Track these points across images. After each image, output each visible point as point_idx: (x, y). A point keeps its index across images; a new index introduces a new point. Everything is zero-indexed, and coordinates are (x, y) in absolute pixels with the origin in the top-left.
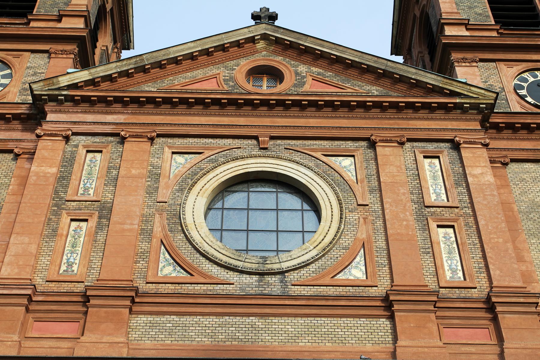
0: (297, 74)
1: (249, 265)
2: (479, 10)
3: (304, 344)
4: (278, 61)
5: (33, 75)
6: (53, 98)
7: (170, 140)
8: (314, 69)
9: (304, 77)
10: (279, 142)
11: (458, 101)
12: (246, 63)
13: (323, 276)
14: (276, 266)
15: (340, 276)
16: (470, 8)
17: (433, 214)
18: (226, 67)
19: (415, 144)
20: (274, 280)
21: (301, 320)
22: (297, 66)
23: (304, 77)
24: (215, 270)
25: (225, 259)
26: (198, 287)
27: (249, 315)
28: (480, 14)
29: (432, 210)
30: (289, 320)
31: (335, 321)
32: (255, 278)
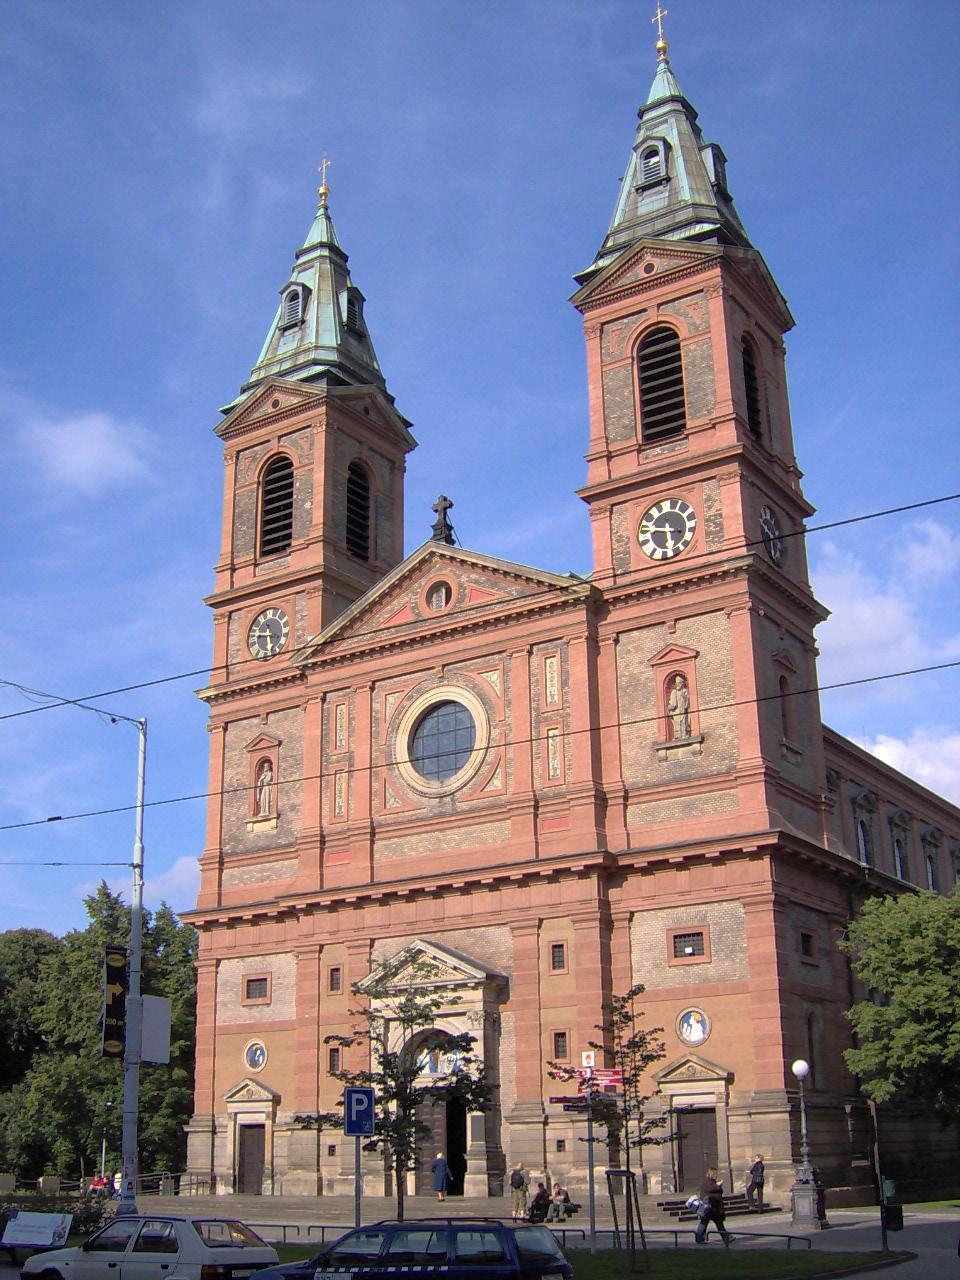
0: (460, 586)
1: (434, 791)
2: (626, 421)
3: (464, 847)
4: (448, 574)
5: (302, 619)
6: (305, 666)
7: (383, 683)
8: (473, 576)
9: (465, 589)
10: (451, 666)
11: (563, 599)
12: (425, 582)
13: (475, 792)
14: (448, 788)
15: (487, 789)
16: (619, 418)
17: (546, 719)
18: (412, 592)
19: (541, 646)
20: (448, 799)
21: (463, 830)
22: (459, 577)
23: (465, 589)
24: (415, 797)
25: (420, 788)
26: (407, 814)
27: (434, 831)
28: (625, 427)
29: (545, 715)
30: (456, 831)
31: (480, 827)
32: (438, 800)
